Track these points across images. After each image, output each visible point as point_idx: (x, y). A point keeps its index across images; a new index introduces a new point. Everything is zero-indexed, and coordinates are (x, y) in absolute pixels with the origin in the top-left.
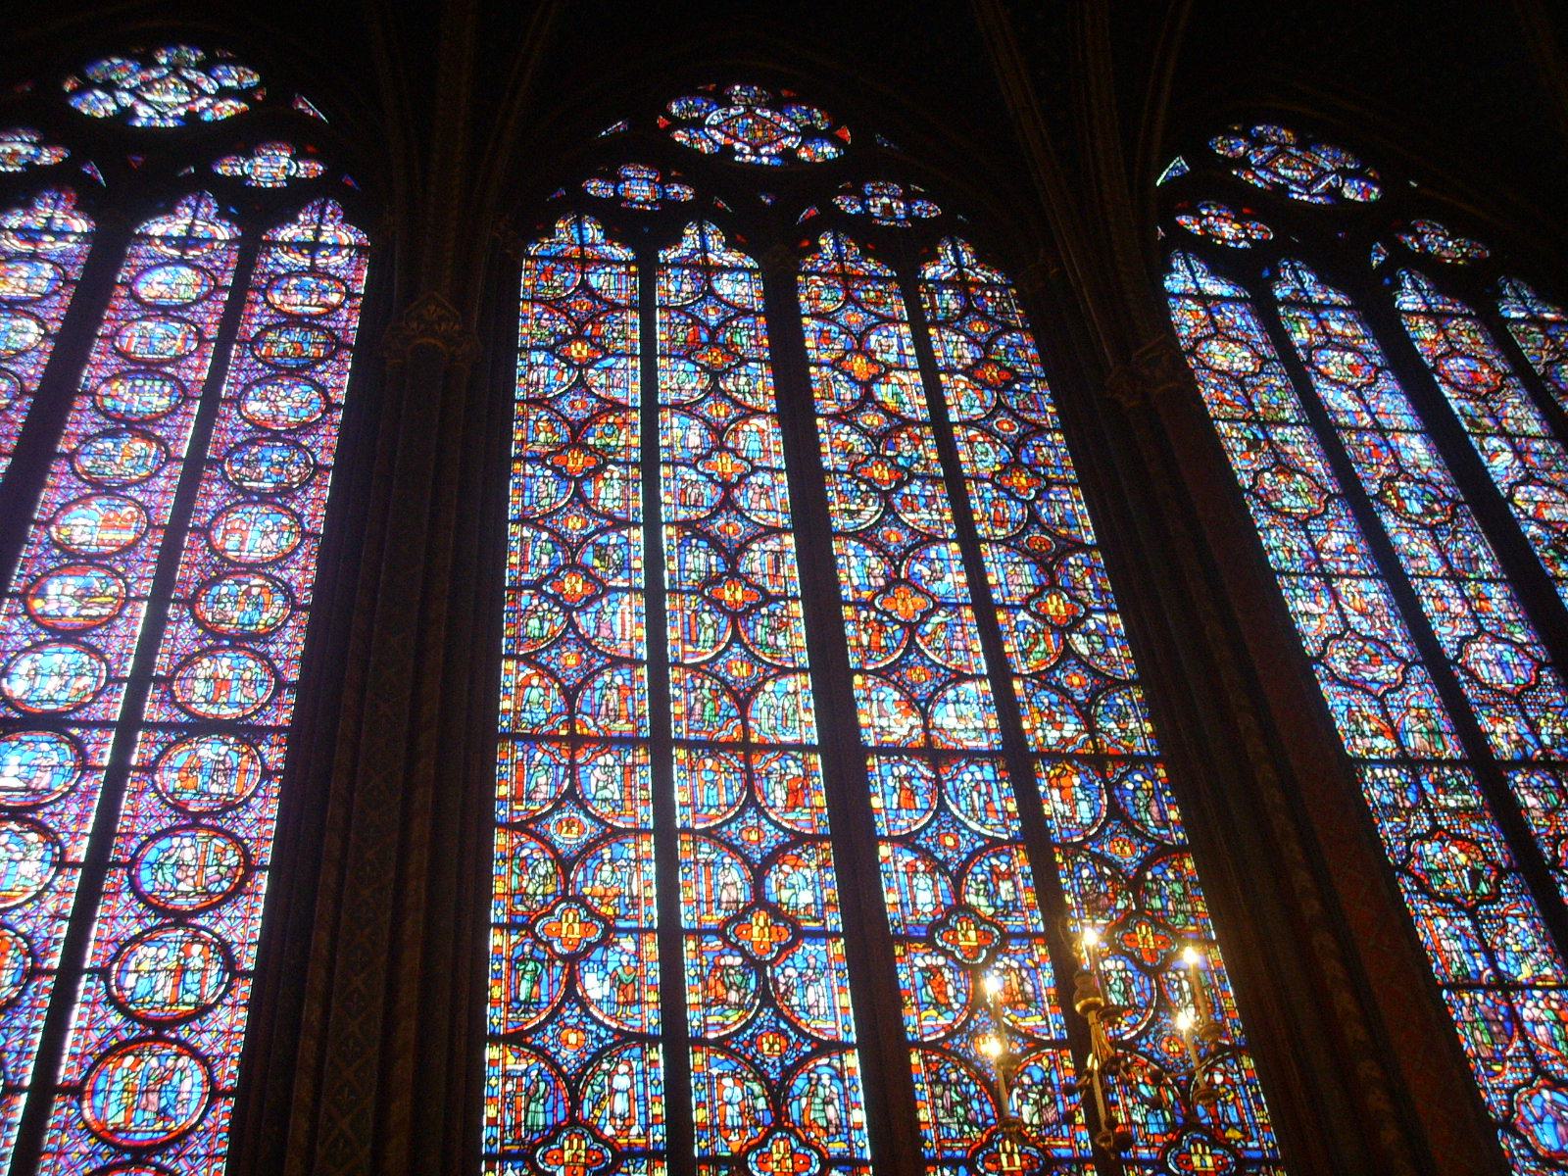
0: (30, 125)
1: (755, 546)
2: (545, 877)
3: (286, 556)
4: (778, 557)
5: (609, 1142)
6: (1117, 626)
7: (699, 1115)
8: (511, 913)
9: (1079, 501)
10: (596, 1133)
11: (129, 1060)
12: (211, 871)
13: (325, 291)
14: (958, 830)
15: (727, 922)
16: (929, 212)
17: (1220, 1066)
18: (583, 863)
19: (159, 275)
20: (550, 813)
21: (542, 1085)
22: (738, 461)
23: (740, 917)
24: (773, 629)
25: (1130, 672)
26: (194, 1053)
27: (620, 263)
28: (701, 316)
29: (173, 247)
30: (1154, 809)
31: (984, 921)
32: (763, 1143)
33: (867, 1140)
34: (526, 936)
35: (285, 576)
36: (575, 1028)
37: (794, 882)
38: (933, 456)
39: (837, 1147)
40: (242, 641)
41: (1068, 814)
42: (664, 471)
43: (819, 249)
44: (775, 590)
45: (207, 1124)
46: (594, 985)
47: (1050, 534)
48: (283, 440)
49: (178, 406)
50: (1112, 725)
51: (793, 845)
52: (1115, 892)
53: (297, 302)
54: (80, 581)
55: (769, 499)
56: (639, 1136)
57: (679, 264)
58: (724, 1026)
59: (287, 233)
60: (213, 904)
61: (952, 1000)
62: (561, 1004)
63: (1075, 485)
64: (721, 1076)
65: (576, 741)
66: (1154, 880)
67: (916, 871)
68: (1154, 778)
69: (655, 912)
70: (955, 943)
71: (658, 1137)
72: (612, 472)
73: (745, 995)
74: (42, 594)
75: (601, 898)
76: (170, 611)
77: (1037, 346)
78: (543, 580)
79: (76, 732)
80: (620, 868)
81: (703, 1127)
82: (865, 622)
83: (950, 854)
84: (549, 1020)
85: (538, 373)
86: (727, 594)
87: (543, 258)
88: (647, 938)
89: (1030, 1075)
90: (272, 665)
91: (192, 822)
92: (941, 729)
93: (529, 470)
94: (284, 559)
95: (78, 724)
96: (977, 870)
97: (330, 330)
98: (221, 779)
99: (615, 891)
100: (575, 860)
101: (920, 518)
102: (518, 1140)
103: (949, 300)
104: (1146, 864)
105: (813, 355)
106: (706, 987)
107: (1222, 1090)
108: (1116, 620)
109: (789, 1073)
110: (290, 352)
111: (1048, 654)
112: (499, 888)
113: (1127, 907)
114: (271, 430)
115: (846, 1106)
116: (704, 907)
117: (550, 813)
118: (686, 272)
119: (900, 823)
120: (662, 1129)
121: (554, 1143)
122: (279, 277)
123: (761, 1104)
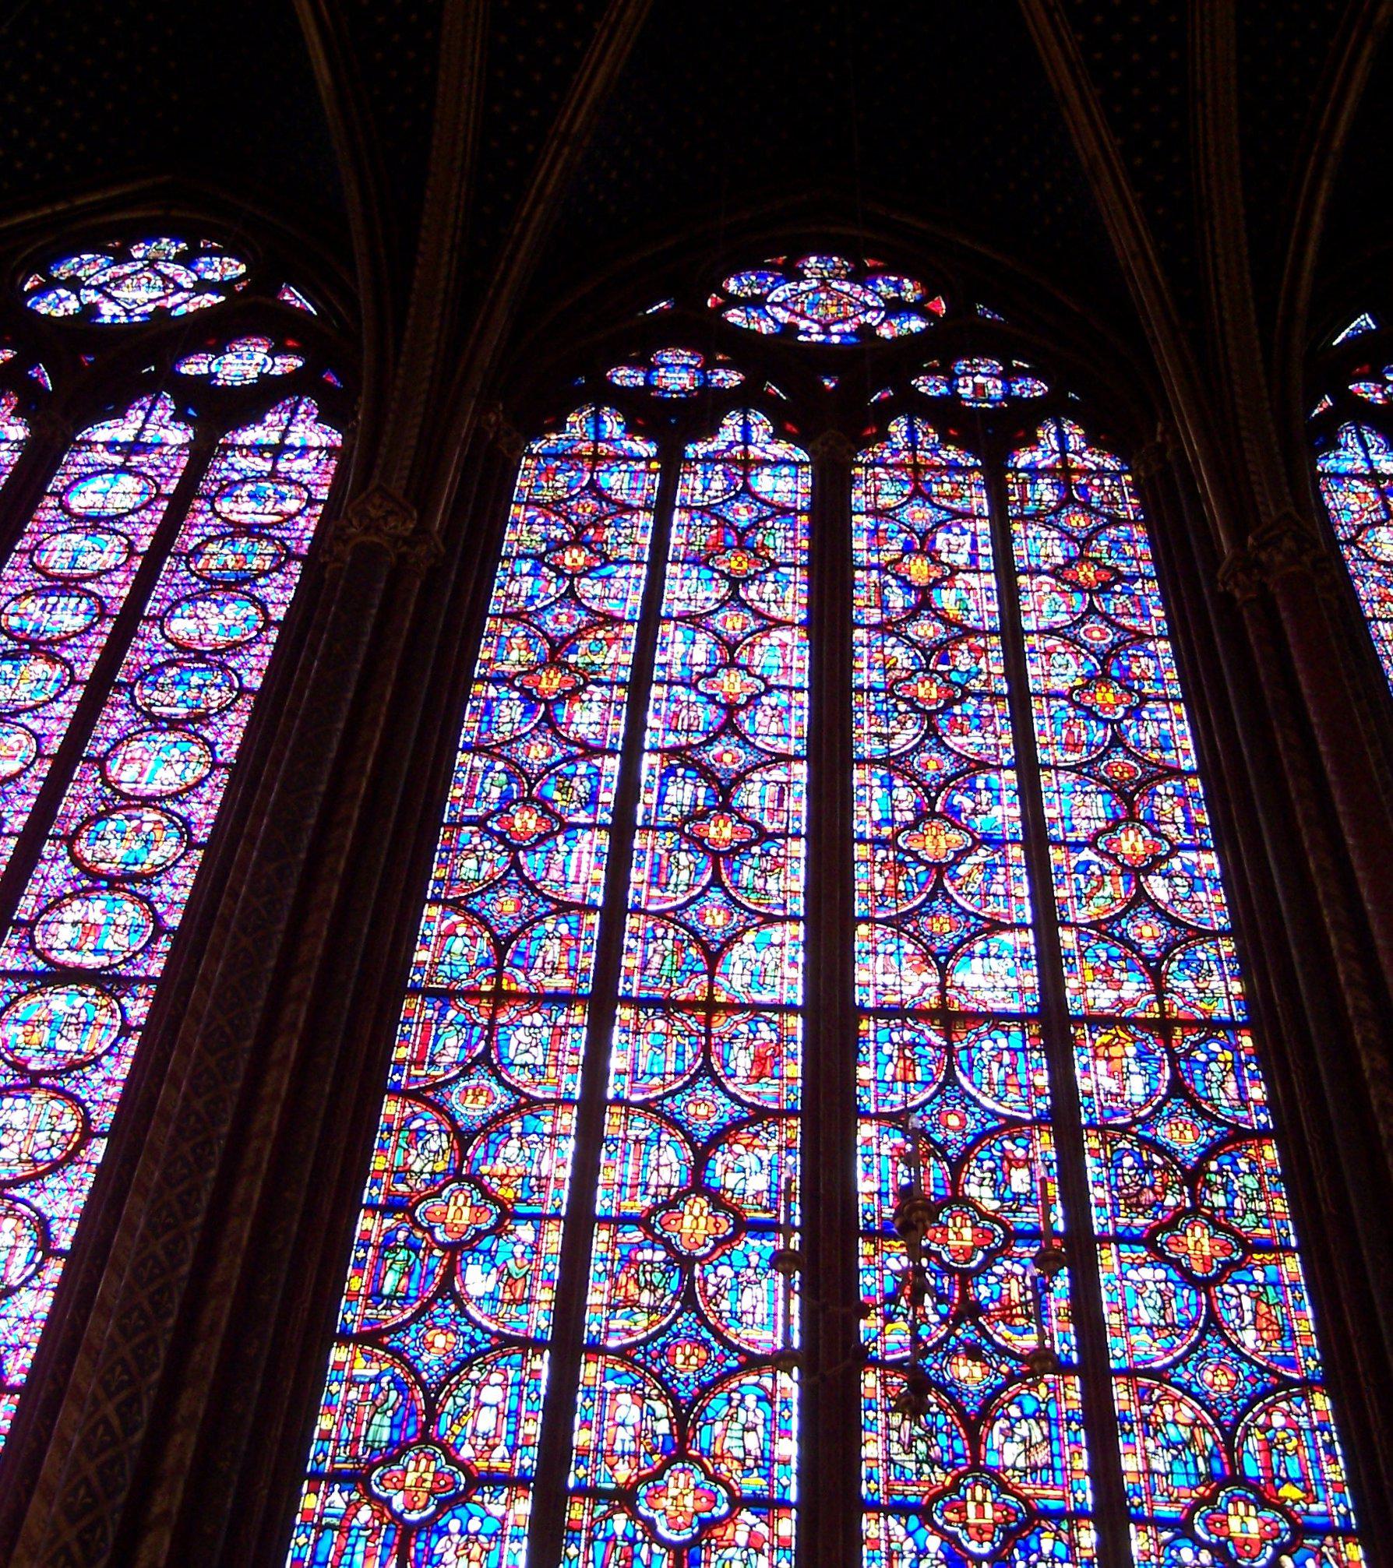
1: (756, 776)
2: (437, 1153)
3: (189, 788)
4: (783, 789)
5: (464, 1466)
6: (1211, 867)
7: (582, 1438)
9: (1180, 720)
10: (450, 1453)
12: (41, 1138)
13: (283, 498)
14: (966, 1108)
15: (652, 1211)
16: (1033, 390)
17: (1283, 1405)
19: (97, 483)
20: (455, 1079)
21: (393, 1394)
22: (750, 680)
23: (670, 1205)
24: (764, 871)
25: (1222, 922)
27: (639, 459)
28: (730, 517)
29: (117, 453)
30: (1231, 1087)
31: (984, 1216)
32: (658, 1474)
33: (794, 1478)
34: (403, 1220)
35: (183, 811)
36: (445, 1329)
37: (745, 1165)
38: (999, 670)
39: (753, 1484)
41: (1115, 1090)
42: (656, 691)
43: (887, 437)
44: (770, 827)
46: (477, 1280)
47: (1136, 758)
48: (207, 661)
49: (92, 625)
50: (1189, 984)
51: (750, 1121)
52: (1165, 1186)
56: (503, 1460)
57: (710, 459)
59: (247, 436)
61: (929, 1311)
62: (432, 1301)
63: (1176, 701)
64: (617, 1392)
66: (1220, 1172)
68: (1235, 1049)
70: (944, 1242)
71: (527, 1462)
72: (592, 693)
73: (663, 1296)
75: (502, 1177)
76: (46, 848)
77: (1151, 542)
78: (490, 815)
80: (529, 1143)
81: (584, 1452)
82: (882, 863)
83: (951, 1135)
84: (415, 1318)
85: (517, 584)
86: (713, 832)
87: (546, 456)
88: (551, 1226)
89: (1020, 1405)
90: (153, 909)
93: (492, 692)
96: (984, 1155)
97: (282, 540)
98: (72, 1035)
99: (520, 1170)
100: (477, 1133)
101: (969, 743)
103: (1046, 492)
104: (1211, 1151)
105: (862, 558)
106: (616, 1286)
107: (1281, 1435)
108: (1211, 859)
109: (706, 1390)
110: (231, 564)
111: (1114, 899)
112: (379, 1163)
113: (1178, 1205)
114: (195, 651)
115: (772, 1433)
116: (627, 1191)
117: (455, 1079)
118: (719, 467)
119: (892, 1097)
120: (534, 1452)
121: (397, 1463)
122: (233, 484)
123: (663, 1427)
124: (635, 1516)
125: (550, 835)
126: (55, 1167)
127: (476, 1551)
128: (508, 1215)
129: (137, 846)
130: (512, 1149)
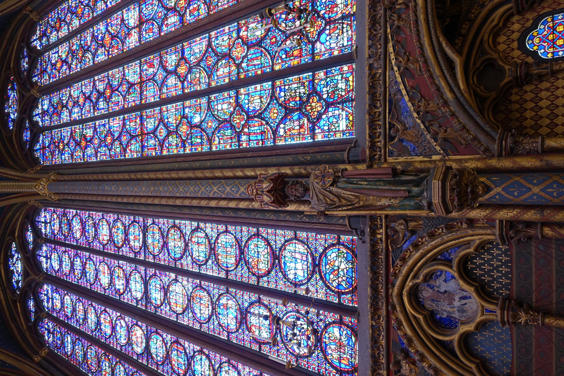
0: (27, 302)
3: (107, 223)
5: (234, 109)
8: (181, 148)
11: (220, 257)
15: (180, 81)
18: (169, 127)
21: (221, 132)
26: (217, 238)
32: (233, 59)
35: (112, 222)
36: (208, 124)
39: (234, 35)
40: (126, 234)
45: (234, 232)
46: (197, 120)
53: (57, 227)
54: (116, 279)
55: (86, 86)
57: (42, 121)
58: (205, 77)
59: (43, 231)
60: (183, 235)
62: (201, 129)
64: (217, 76)
65: (142, 134)
67: (167, 24)
69: (179, 103)
74: (119, 290)
79: (148, 278)
81: (230, 79)
84: (205, 132)
91: (165, 245)
92: (135, 23)
93: (86, 157)
94: (108, 223)
95: (146, 276)
102: (234, 137)
105: (57, 78)
106: (196, 84)
112: (175, 152)
117: (158, 139)
123: (224, 61)
124: (242, 62)
125: (111, 132)
126: (181, 232)
127: (252, 99)
128: (184, 116)
129: (119, 232)
130: (170, 120)
